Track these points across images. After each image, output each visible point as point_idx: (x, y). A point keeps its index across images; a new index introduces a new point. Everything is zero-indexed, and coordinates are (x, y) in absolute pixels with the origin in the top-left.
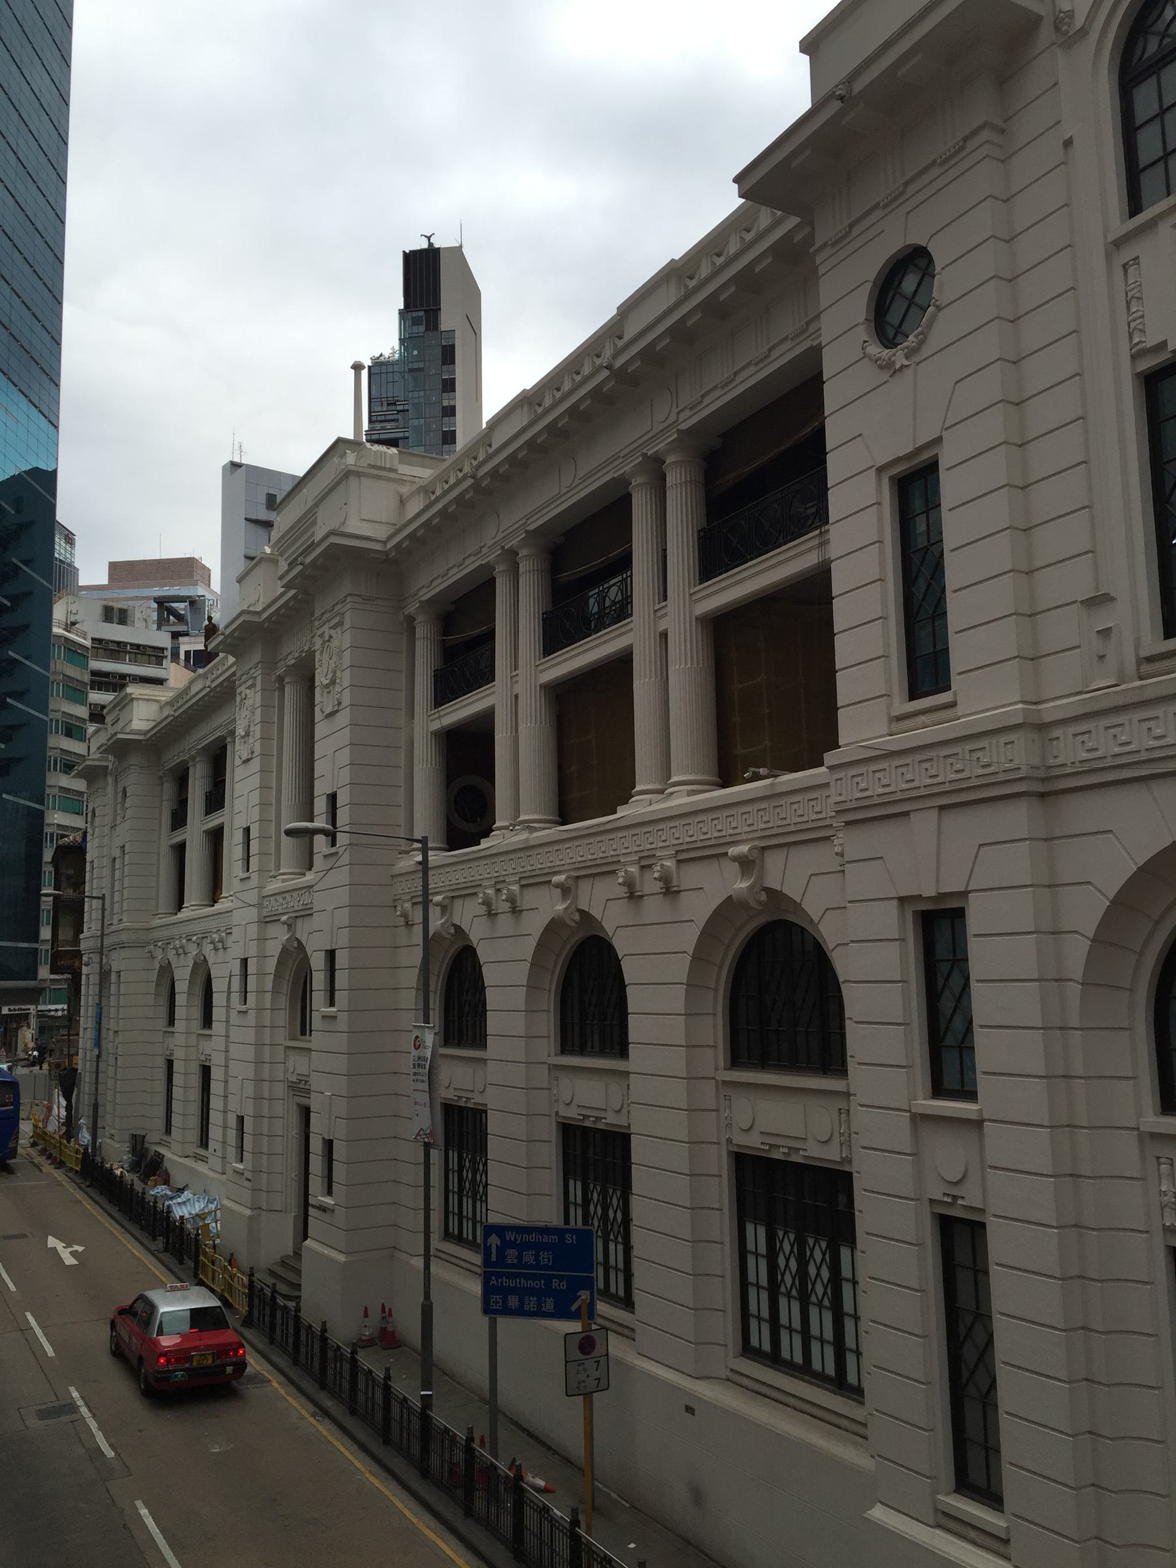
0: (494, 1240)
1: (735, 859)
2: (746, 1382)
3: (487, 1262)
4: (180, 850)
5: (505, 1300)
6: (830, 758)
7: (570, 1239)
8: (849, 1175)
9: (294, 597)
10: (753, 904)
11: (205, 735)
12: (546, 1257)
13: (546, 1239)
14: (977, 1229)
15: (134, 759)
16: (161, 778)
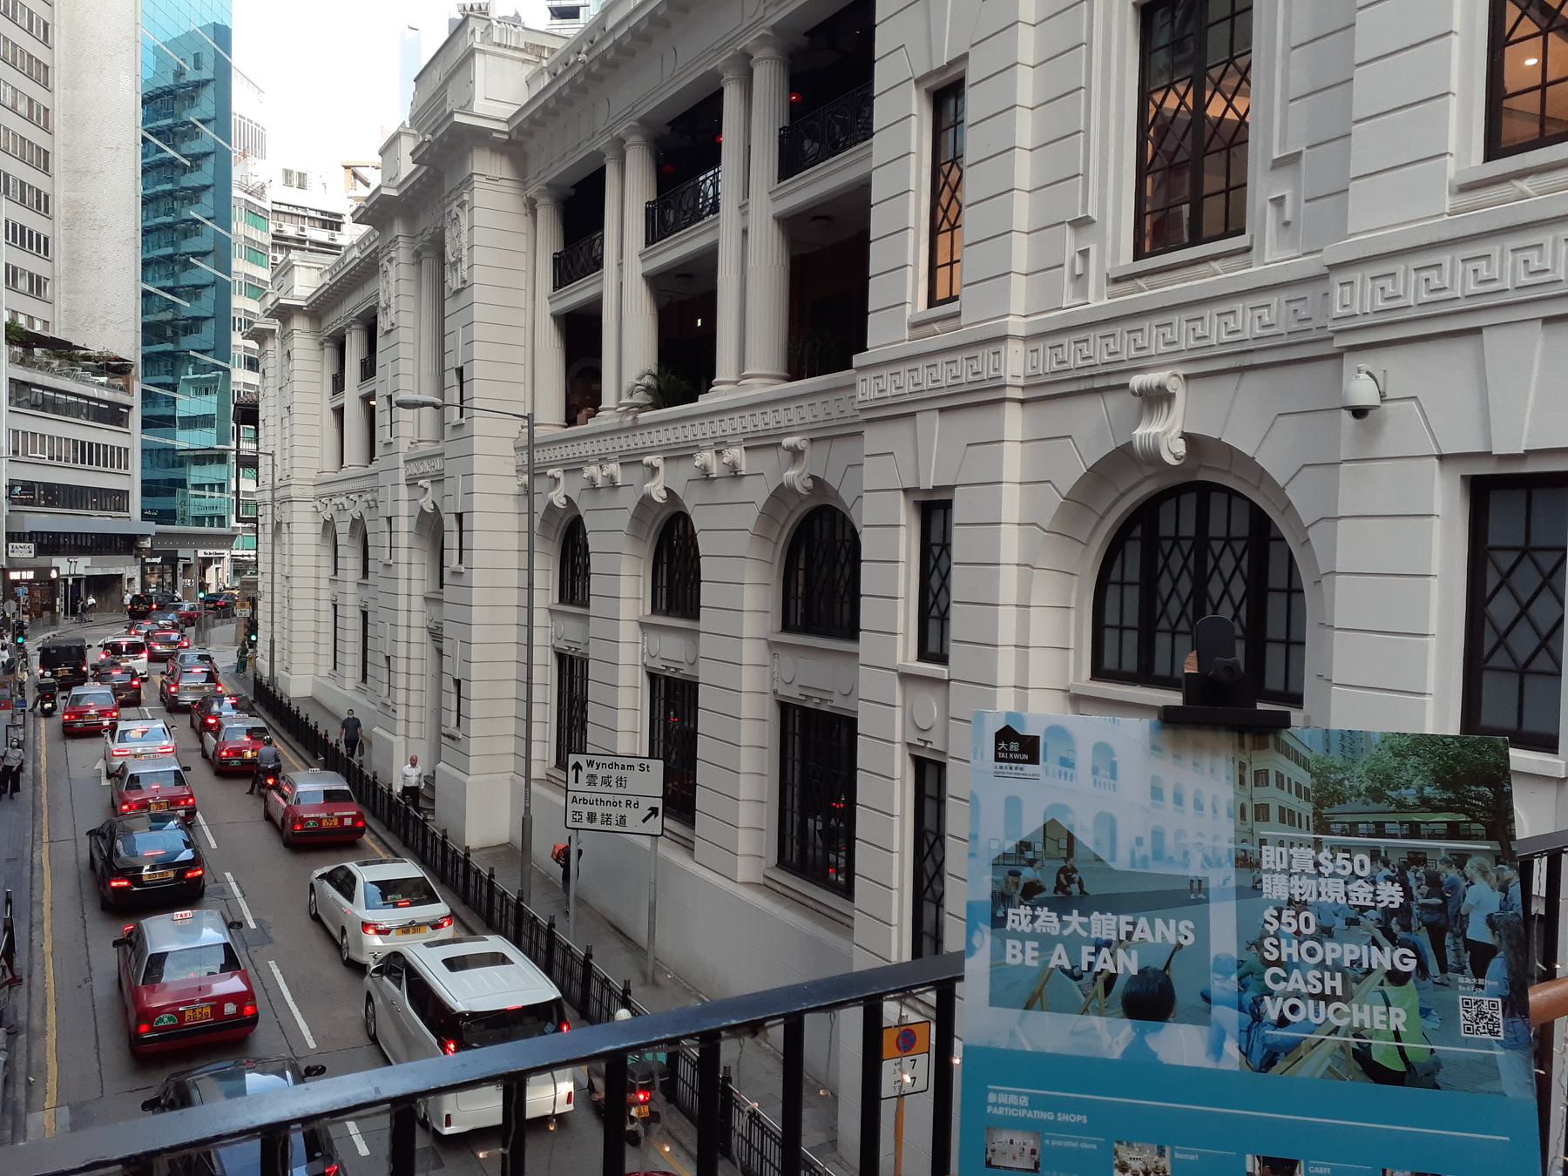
1: (789, 449)
2: (778, 887)
4: (339, 412)
6: (858, 360)
8: (852, 722)
9: (426, 173)
10: (800, 489)
11: (354, 305)
14: (941, 767)
15: (299, 324)
16: (322, 344)
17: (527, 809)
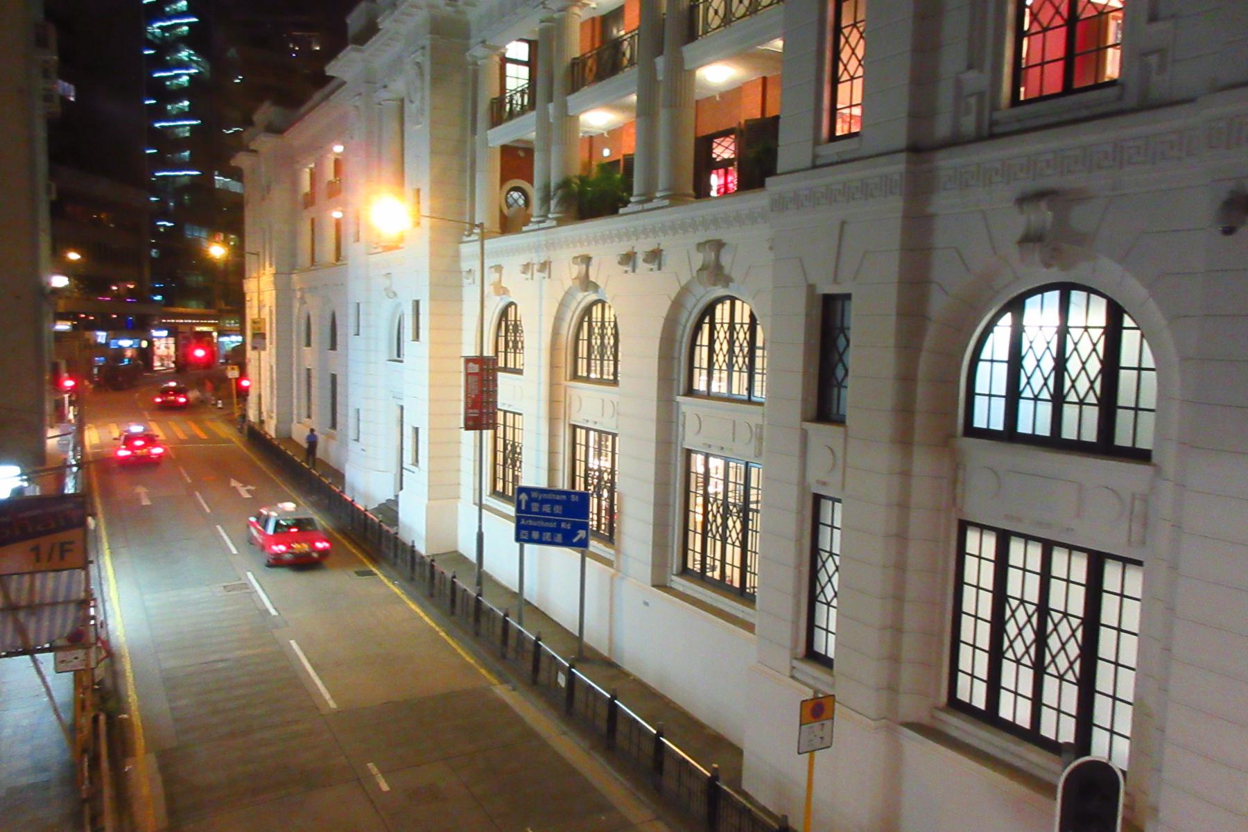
0: (524, 497)
3: (518, 510)
5: (530, 534)
7: (574, 498)
12: (558, 509)
13: (558, 497)
17: (480, 527)
